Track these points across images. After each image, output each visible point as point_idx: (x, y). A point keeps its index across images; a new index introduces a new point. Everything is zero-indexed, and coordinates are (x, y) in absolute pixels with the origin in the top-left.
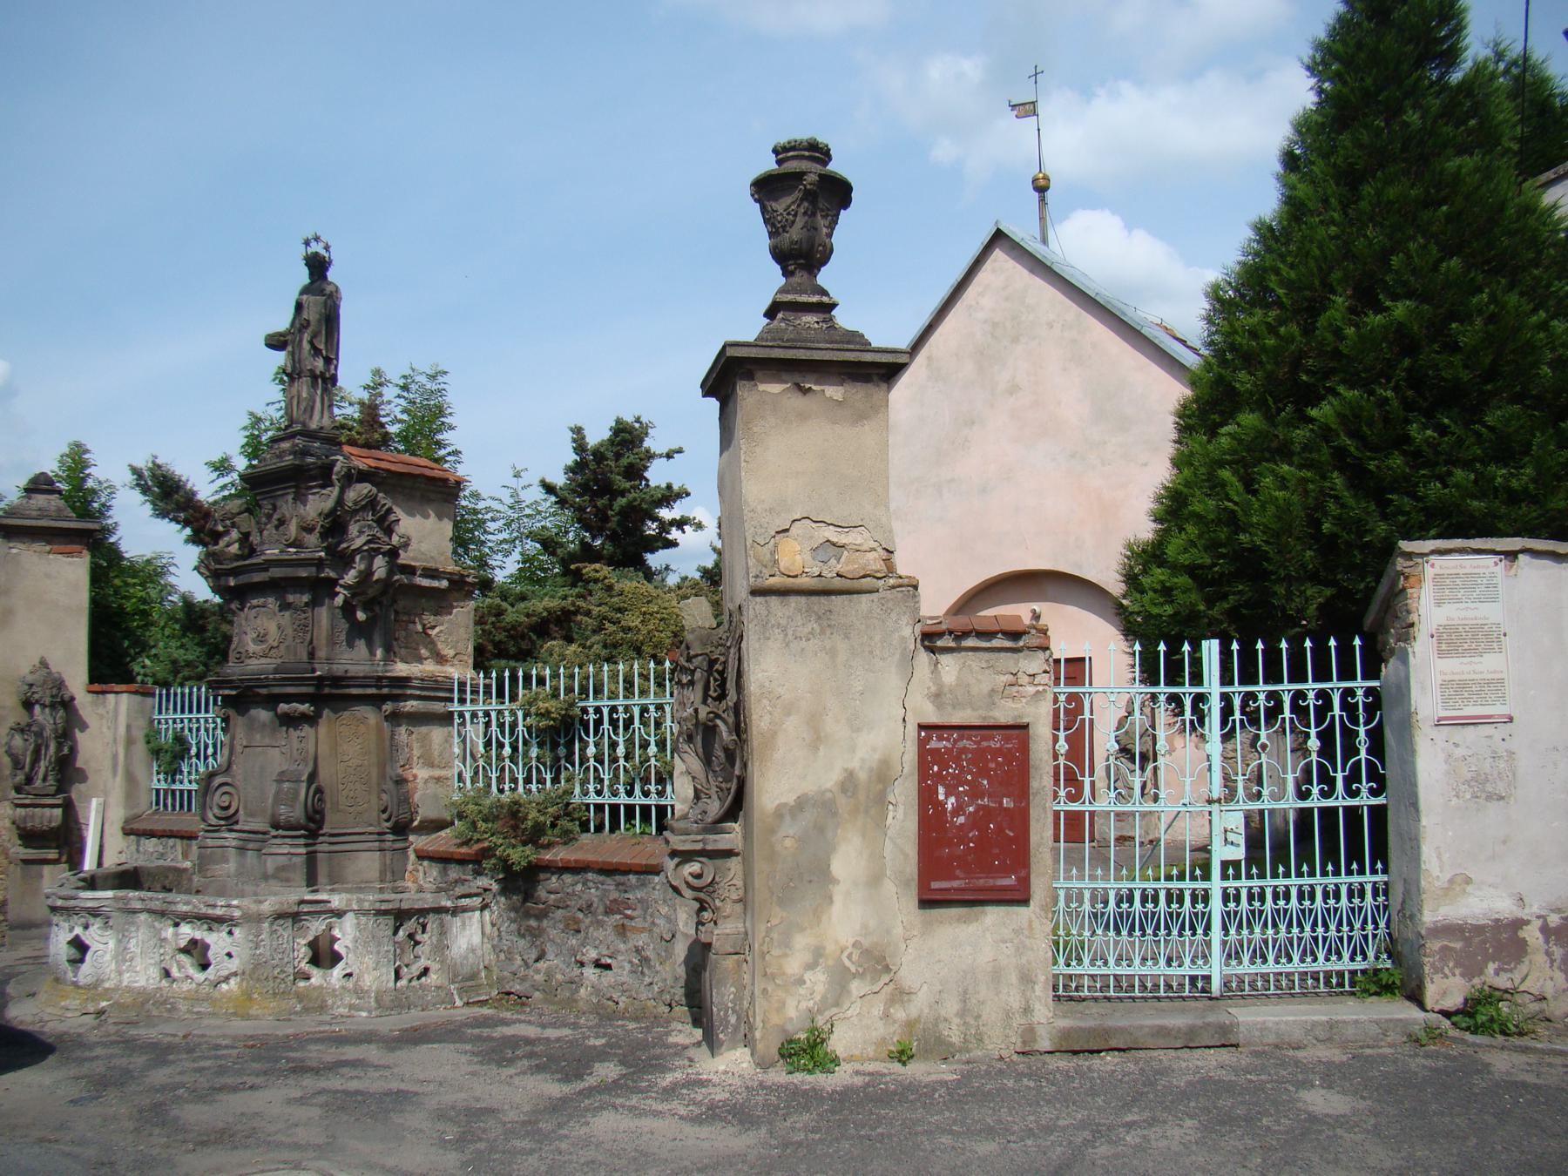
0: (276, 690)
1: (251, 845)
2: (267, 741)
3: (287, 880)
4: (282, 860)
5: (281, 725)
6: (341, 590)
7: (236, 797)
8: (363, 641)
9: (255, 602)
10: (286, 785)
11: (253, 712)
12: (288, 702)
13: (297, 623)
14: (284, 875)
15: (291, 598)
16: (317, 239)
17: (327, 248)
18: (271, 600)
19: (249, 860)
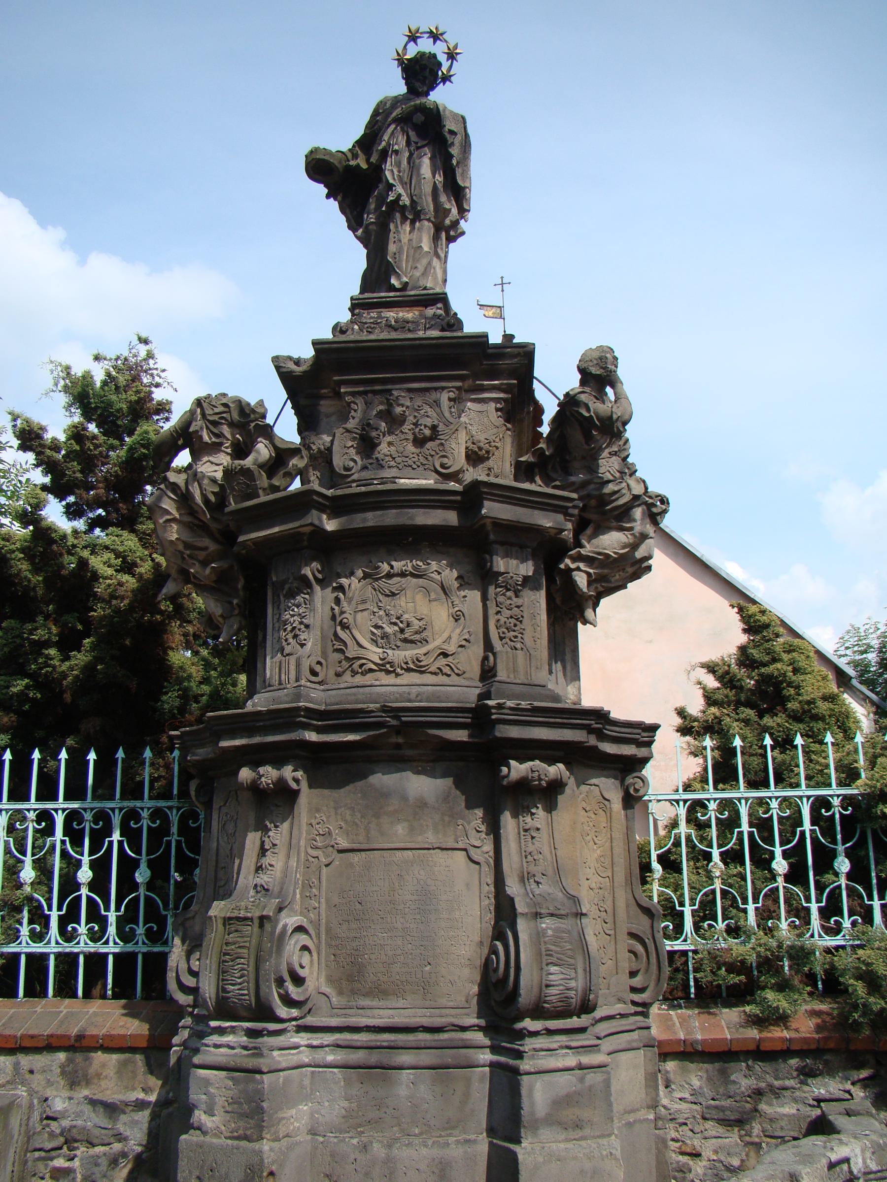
0: (515, 732)
1: (405, 1058)
2: (431, 837)
3: (578, 1125)
4: (565, 1082)
5: (470, 806)
6: (582, 565)
7: (315, 954)
8: (559, 664)
9: (398, 565)
10: (547, 924)
11: (381, 780)
12: (521, 760)
13: (508, 613)
14: (569, 1114)
15: (500, 564)
16: (435, 37)
17: (452, 56)
18: (434, 565)
19: (403, 1091)
